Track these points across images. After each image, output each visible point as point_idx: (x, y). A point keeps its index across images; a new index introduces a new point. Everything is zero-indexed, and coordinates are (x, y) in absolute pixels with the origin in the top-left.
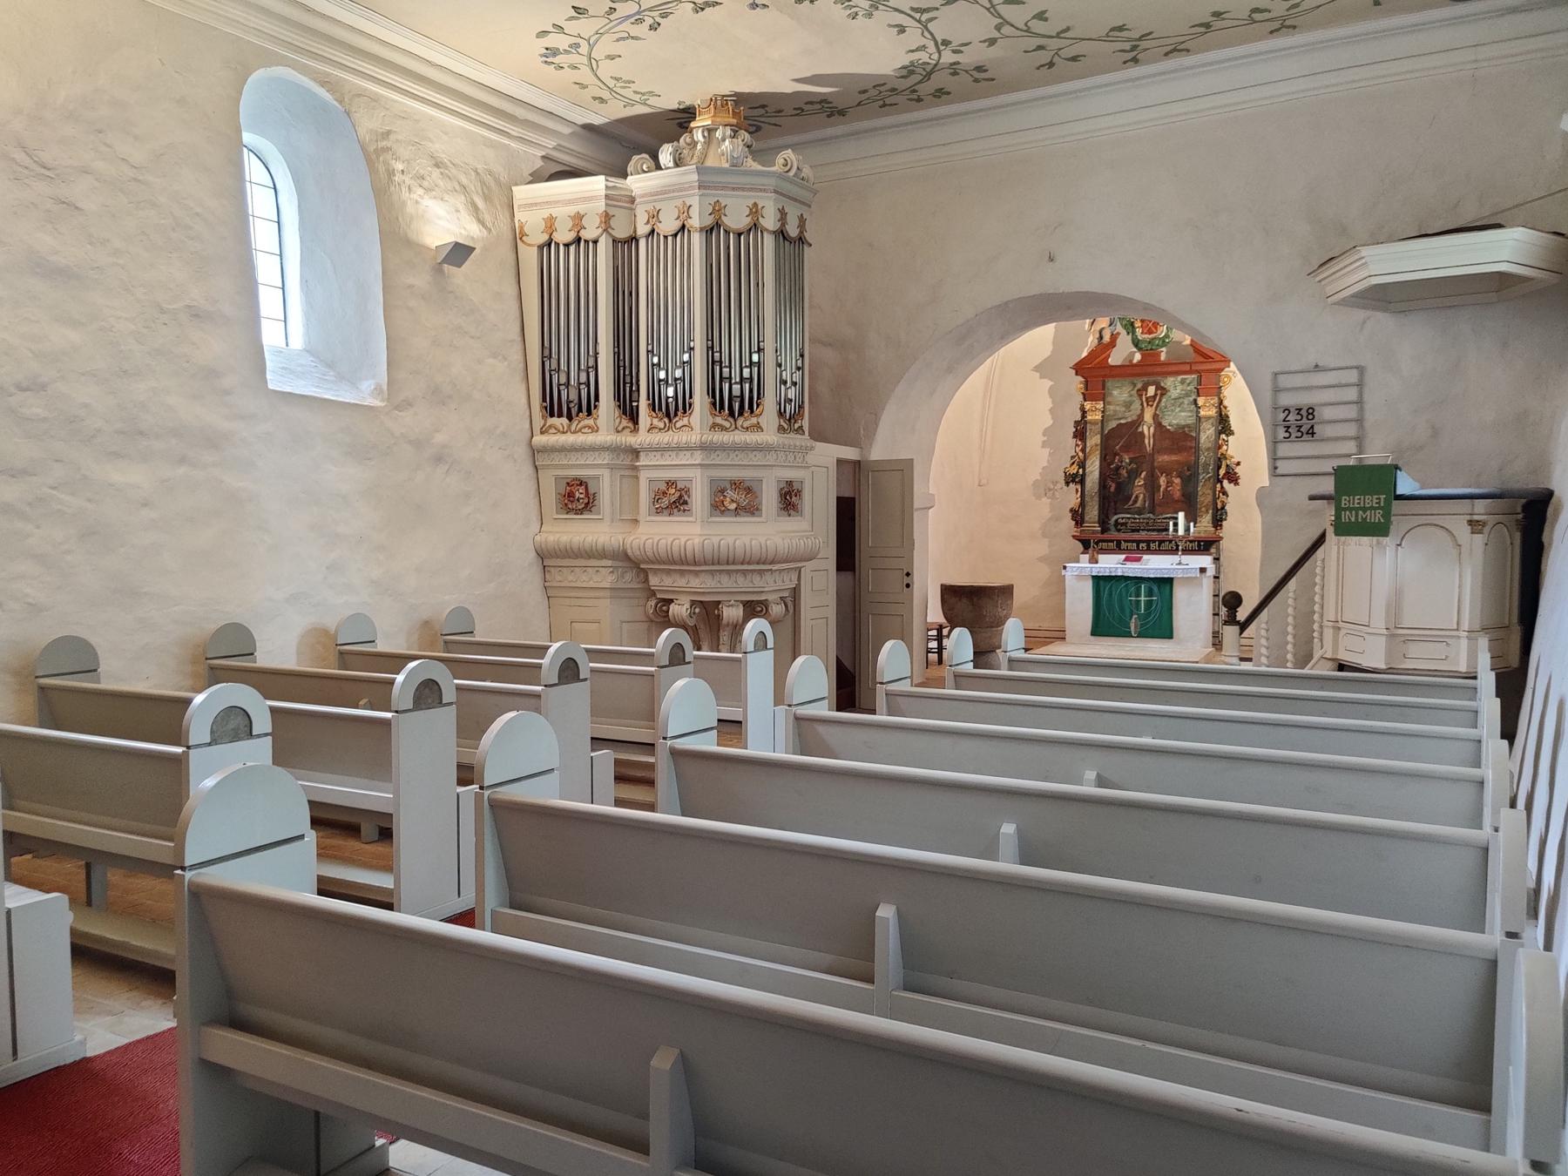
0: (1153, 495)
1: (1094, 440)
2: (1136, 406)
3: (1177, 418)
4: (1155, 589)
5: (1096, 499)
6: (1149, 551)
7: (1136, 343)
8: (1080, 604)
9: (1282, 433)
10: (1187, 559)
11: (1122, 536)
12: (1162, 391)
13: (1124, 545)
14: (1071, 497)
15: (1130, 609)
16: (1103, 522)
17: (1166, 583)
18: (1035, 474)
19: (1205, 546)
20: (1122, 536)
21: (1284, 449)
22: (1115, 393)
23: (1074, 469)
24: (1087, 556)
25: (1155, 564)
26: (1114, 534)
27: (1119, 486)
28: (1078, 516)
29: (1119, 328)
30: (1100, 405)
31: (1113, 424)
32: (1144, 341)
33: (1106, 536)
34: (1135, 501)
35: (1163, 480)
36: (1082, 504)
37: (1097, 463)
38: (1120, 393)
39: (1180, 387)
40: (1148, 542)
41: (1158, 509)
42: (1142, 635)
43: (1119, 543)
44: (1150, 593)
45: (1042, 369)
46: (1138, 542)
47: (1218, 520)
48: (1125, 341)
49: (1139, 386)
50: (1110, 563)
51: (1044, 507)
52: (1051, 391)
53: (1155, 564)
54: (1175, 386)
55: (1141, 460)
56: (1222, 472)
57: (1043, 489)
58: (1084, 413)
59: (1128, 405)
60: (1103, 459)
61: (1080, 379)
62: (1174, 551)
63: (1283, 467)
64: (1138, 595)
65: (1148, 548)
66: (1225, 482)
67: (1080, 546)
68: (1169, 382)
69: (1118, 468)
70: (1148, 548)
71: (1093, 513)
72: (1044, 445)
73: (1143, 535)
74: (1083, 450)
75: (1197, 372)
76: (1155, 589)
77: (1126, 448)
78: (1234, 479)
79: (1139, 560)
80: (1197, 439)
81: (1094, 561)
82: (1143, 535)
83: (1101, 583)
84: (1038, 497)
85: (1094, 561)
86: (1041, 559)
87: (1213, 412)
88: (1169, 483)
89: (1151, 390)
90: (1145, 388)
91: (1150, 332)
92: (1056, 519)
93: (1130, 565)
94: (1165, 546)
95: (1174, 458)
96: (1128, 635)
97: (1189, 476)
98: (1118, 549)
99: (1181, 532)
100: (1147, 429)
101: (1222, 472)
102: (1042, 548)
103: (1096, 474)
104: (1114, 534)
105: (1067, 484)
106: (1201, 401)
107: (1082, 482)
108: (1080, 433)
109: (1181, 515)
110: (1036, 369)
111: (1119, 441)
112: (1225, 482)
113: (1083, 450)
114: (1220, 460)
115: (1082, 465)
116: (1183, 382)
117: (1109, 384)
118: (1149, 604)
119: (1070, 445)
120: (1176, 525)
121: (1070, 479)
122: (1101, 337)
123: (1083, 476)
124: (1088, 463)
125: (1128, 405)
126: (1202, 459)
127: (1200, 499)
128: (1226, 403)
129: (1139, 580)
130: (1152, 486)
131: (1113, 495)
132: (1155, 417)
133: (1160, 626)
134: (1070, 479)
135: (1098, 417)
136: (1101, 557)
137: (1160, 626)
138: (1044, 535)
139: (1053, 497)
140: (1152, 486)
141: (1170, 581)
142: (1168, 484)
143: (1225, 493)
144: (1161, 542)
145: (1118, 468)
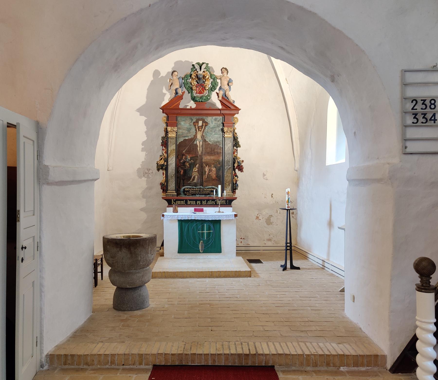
0: (203, 176)
1: (172, 147)
2: (193, 130)
3: (214, 137)
4: (212, 227)
5: (174, 178)
6: (207, 205)
7: (193, 99)
8: (171, 236)
9: (410, 120)
10: (223, 209)
11: (187, 197)
12: (206, 124)
13: (189, 202)
14: (160, 177)
15: (199, 238)
16: (178, 190)
17: (217, 223)
18: (138, 165)
19: (228, 202)
20: (187, 197)
21: (412, 133)
22: (182, 123)
23: (162, 162)
24: (171, 209)
25: (210, 213)
26: (183, 196)
27: (185, 171)
28: (164, 187)
29: (184, 89)
30: (175, 129)
31: (181, 140)
32: (197, 97)
33: (179, 197)
34: (194, 179)
35: (207, 169)
36: (167, 181)
37: (174, 159)
38: (185, 124)
39: (214, 122)
40: (201, 201)
41: (205, 184)
42: (205, 252)
43: (186, 201)
44: (209, 229)
45: (141, 111)
46: (196, 201)
47: (234, 188)
48: (187, 96)
49: (194, 120)
50: (187, 212)
51: (143, 183)
52: (146, 123)
53: (210, 213)
54: (213, 122)
55: (195, 158)
56: (236, 165)
57: (143, 172)
58: (166, 132)
59: (189, 130)
60: (177, 157)
61: (165, 115)
62: (216, 205)
63: (412, 147)
64: (203, 230)
65: (201, 204)
66: (237, 170)
67: (166, 203)
68: (209, 119)
69: (184, 162)
70: (201, 204)
71: (172, 185)
72: (143, 150)
73: (197, 197)
74: (167, 152)
75: (223, 115)
76: (212, 227)
77: (189, 152)
78: (241, 168)
79: (202, 210)
80: (223, 148)
81: (175, 211)
82: (197, 197)
83: (183, 224)
84: (140, 177)
85: (175, 211)
86: (142, 210)
87: (231, 135)
88: (210, 170)
89: (200, 123)
90: (197, 122)
91: (200, 93)
92: (149, 188)
93: (198, 213)
94: (210, 202)
95: (212, 157)
96: (198, 252)
97: (220, 167)
98: (186, 204)
99: (220, 195)
100: (199, 143)
101: (236, 165)
102: (142, 204)
103: (174, 165)
104: (183, 196)
105: (158, 170)
106: (225, 129)
107: (166, 169)
108: (165, 143)
109: (220, 186)
110: (139, 110)
111: (185, 148)
112: (237, 170)
113: (167, 152)
114: (235, 159)
115: (166, 160)
116: (215, 120)
117: (179, 118)
118: (209, 234)
119: (159, 151)
120: (217, 192)
121: (160, 167)
122: (177, 93)
123: (167, 165)
124: (169, 159)
125: (189, 130)
126: (226, 158)
127: (226, 178)
128: (236, 131)
129: (203, 222)
130: (201, 172)
131: (182, 176)
132: (203, 136)
133: (214, 246)
134: (160, 167)
135: (174, 135)
136: (179, 209)
137: (214, 246)
138: (144, 197)
139: (148, 177)
140: (201, 172)
141: (219, 222)
142: (211, 171)
143: (236, 176)
144: (208, 200)
145: (184, 162)
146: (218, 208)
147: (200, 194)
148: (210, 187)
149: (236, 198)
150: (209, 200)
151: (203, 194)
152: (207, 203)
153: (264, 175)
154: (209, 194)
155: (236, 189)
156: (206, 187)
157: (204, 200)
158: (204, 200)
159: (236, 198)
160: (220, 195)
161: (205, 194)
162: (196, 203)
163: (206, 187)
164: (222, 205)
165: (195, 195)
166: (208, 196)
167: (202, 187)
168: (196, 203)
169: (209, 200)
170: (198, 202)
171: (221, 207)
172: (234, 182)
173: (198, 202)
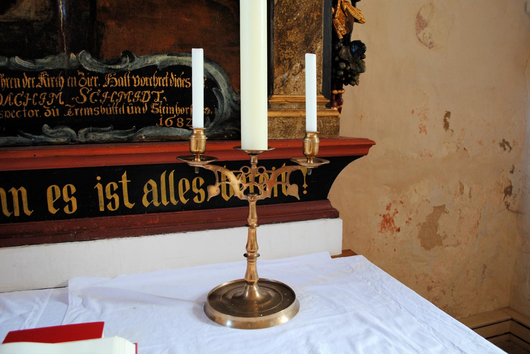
40: (84, 180)
41: (115, 34)
70: (88, 206)
144: (140, 175)
146: (242, 232)
147: (77, 124)
148: (158, 60)
149: (361, 148)
150: (154, 171)
151: (99, 122)
152: (136, 195)
153: (421, 24)
154: (151, 119)
155: (351, 78)
156: (127, 65)
157: (111, 174)
158: (111, 174)
159: (361, 148)
160: (255, 134)
161: (122, 123)
162: (37, 201)
163: (127, 65)
164: (278, 209)
165: (34, 125)
166: (147, 132)
167: (87, 60)
168: (37, 201)
169: (154, 171)
170: (53, 193)
171: (263, 220)
172: (341, 30)
173: (53, 193)
